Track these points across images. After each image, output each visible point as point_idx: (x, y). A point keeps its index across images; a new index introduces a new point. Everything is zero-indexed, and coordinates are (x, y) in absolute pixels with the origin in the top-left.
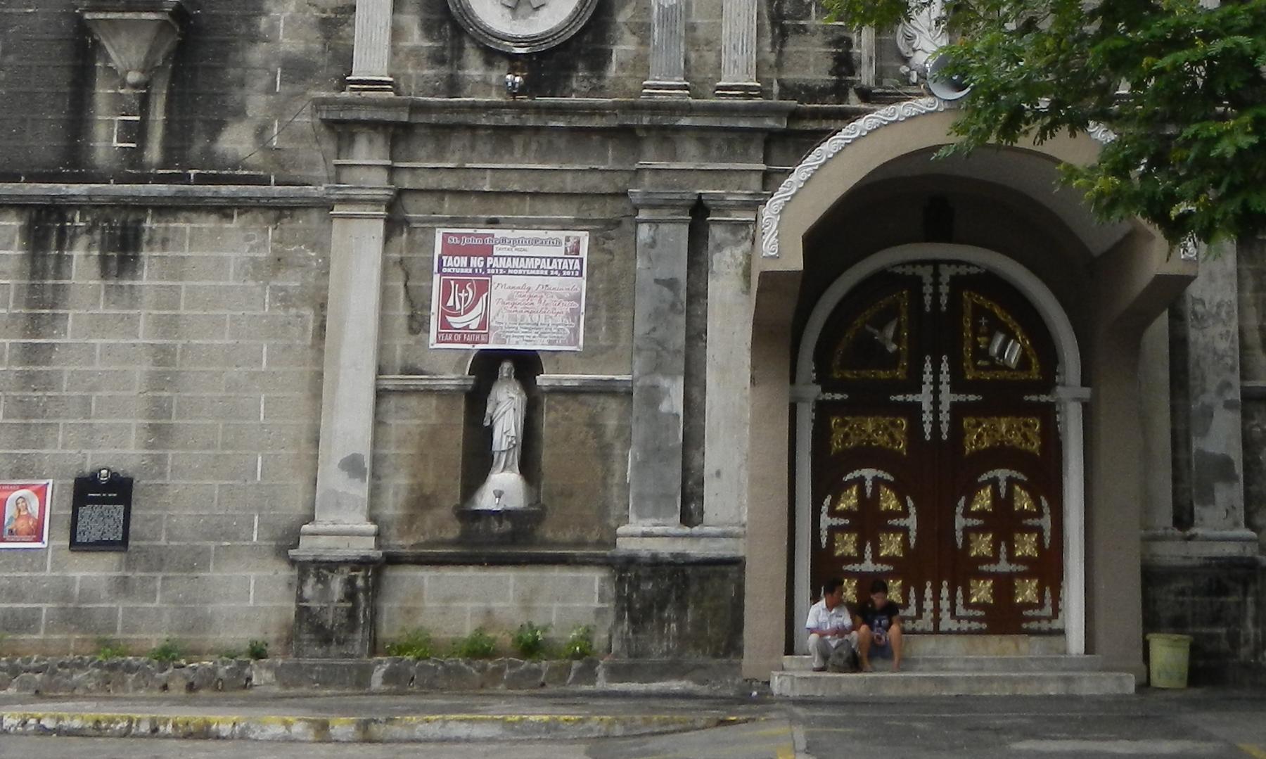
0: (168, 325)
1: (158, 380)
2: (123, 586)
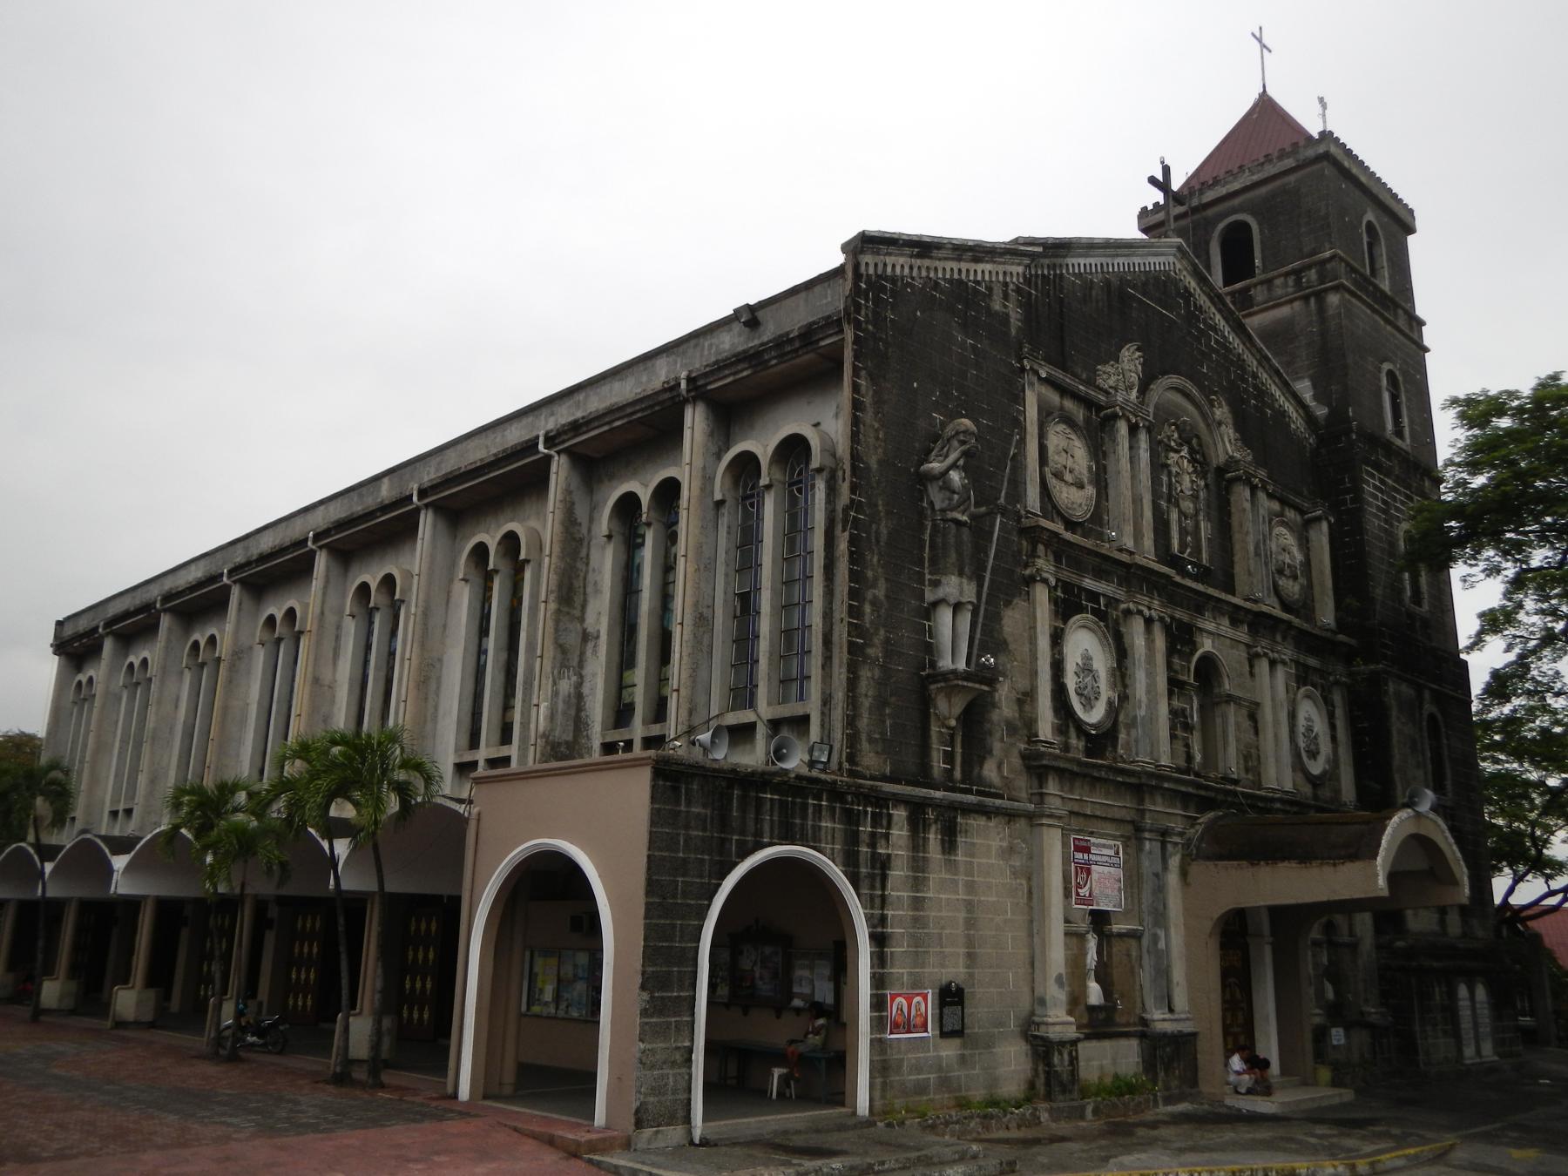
0: (971, 887)
1: (970, 923)
2: (963, 1060)
